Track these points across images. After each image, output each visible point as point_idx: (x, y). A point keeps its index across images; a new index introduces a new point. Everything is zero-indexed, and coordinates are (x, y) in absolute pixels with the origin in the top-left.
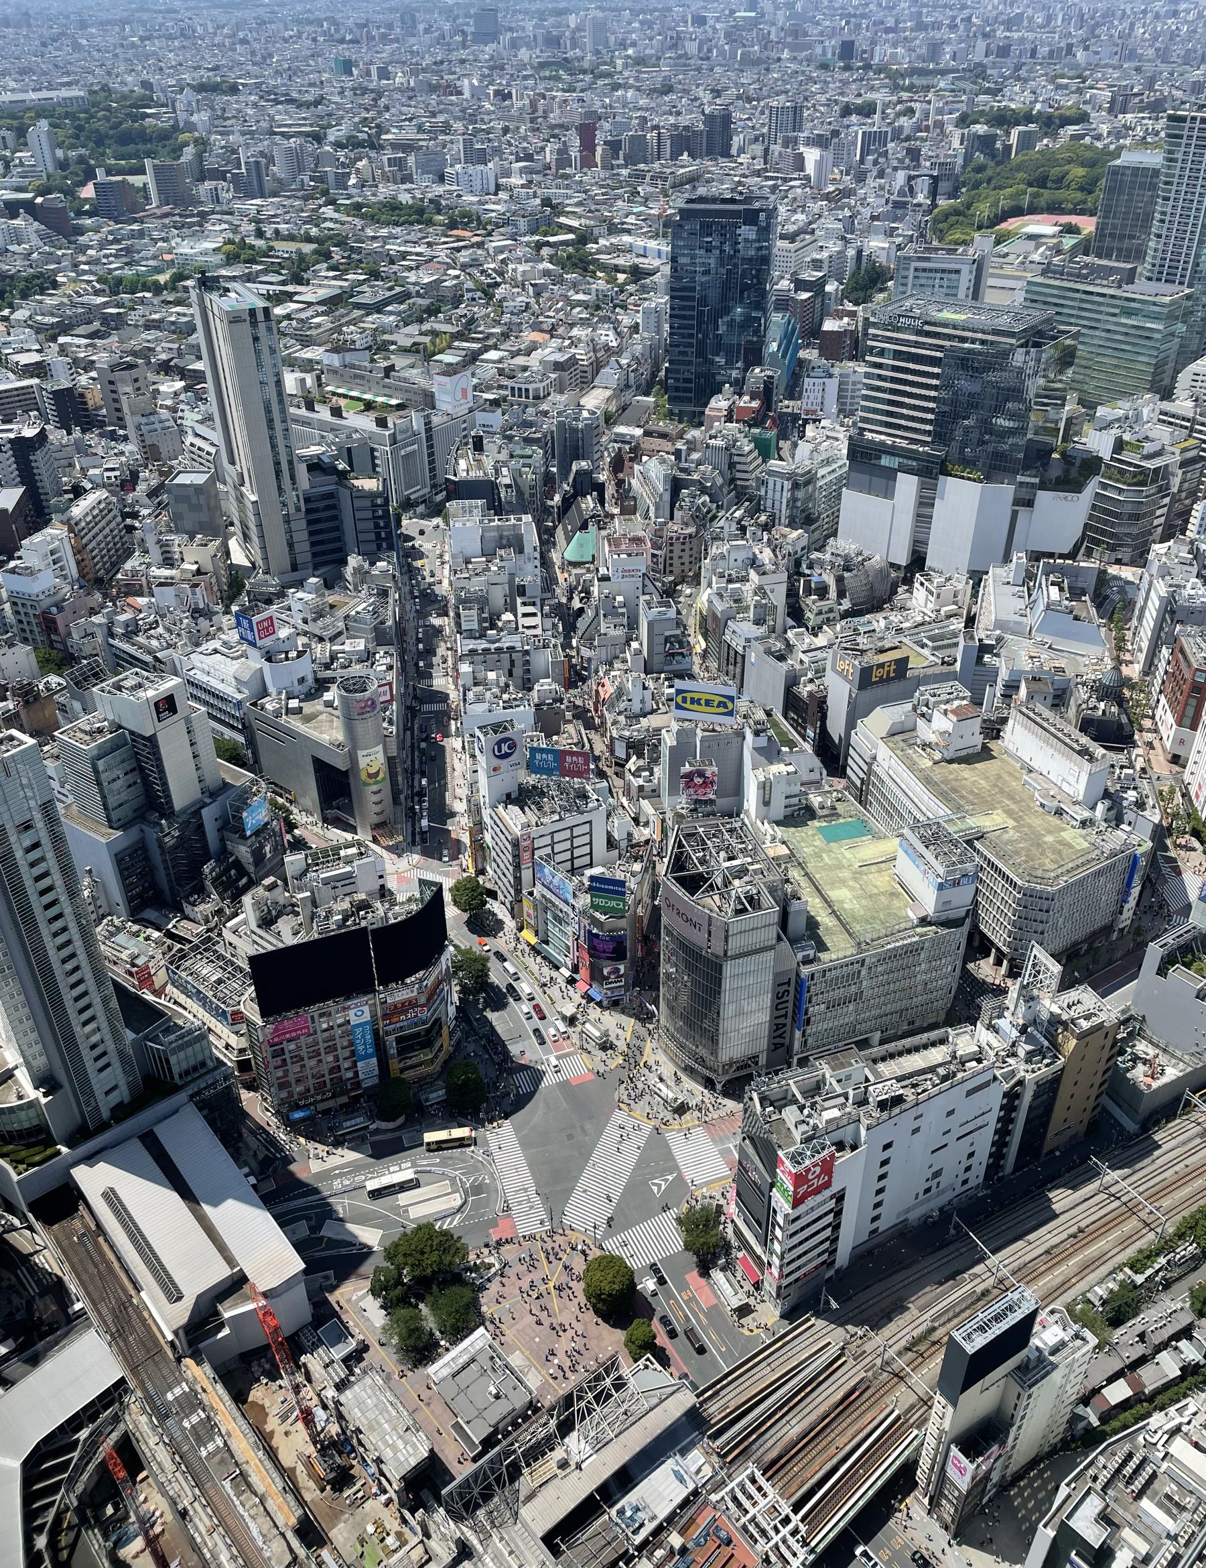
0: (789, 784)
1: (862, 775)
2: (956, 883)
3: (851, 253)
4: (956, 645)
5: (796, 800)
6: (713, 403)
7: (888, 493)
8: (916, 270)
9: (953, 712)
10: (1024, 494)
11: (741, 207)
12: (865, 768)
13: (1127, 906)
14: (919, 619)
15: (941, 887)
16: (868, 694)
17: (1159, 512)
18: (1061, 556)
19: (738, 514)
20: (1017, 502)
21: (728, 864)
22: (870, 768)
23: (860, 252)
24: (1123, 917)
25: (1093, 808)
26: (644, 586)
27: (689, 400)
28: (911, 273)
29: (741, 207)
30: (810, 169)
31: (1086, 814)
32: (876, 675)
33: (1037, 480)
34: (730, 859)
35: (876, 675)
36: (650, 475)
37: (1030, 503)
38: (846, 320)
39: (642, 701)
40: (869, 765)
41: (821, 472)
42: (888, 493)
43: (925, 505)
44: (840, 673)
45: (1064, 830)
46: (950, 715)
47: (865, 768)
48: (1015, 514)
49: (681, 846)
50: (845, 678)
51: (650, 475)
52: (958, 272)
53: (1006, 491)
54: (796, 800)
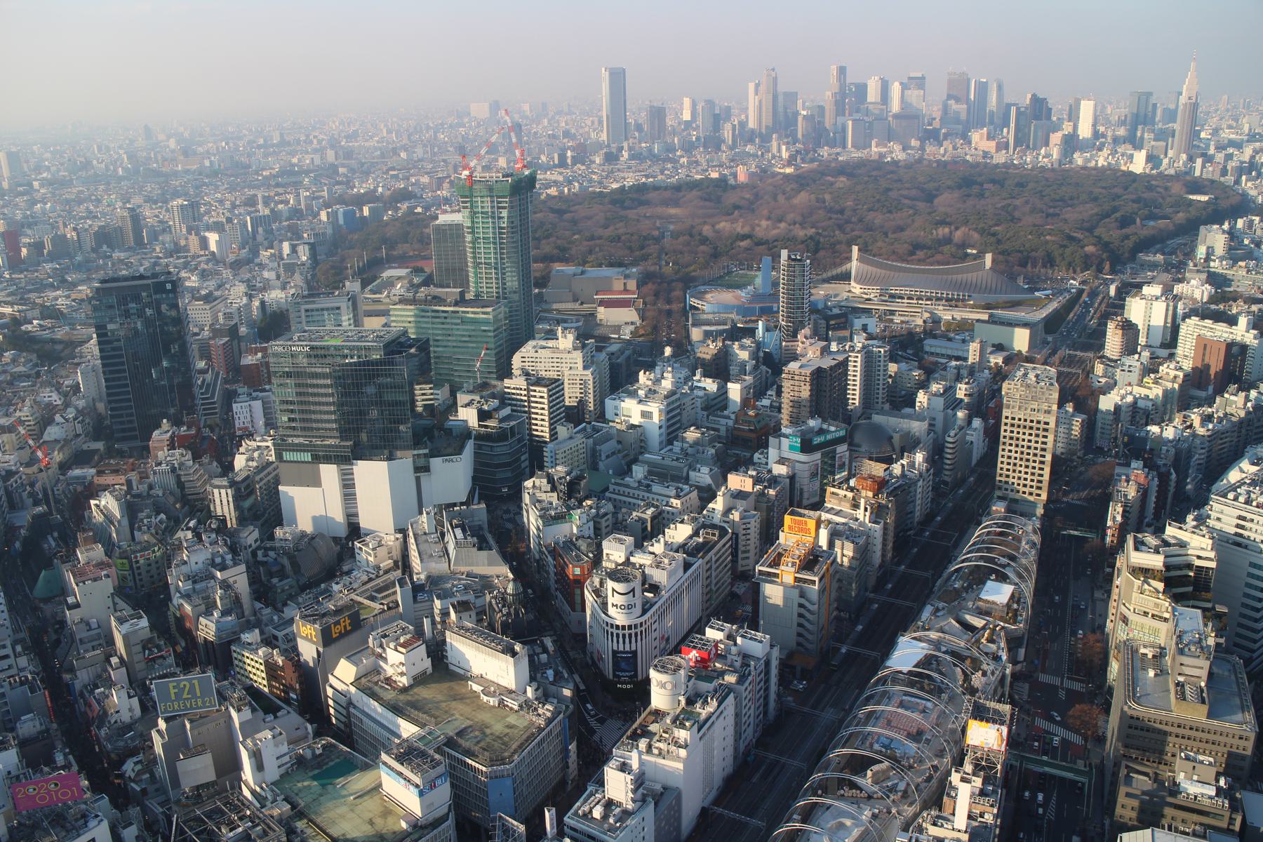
0: (276, 745)
1: (343, 719)
2: (432, 786)
3: (256, 303)
4: (395, 593)
5: (287, 759)
6: (156, 434)
7: (316, 482)
8: (307, 311)
9: (402, 645)
10: (422, 462)
11: (149, 282)
12: (344, 712)
13: (570, 761)
14: (365, 578)
15: (421, 794)
16: (333, 648)
17: (523, 458)
18: (462, 504)
19: (192, 524)
20: (417, 469)
21: (231, 834)
22: (348, 712)
23: (263, 303)
24: (570, 770)
25: (525, 692)
26: (115, 604)
27: (135, 438)
28: (303, 314)
29: (149, 282)
30: (213, 247)
31: (522, 699)
32: (335, 632)
33: (426, 451)
34: (231, 830)
35: (335, 632)
36: (107, 504)
37: (427, 469)
38: (260, 355)
39: (131, 710)
40: (347, 709)
41: (257, 478)
42: (316, 482)
43: (348, 486)
44: (306, 638)
45: (507, 716)
46: (400, 649)
47: (344, 712)
48: (418, 480)
49: (182, 832)
50: (311, 641)
51: (107, 504)
52: (338, 308)
53: (406, 461)
54: (287, 759)
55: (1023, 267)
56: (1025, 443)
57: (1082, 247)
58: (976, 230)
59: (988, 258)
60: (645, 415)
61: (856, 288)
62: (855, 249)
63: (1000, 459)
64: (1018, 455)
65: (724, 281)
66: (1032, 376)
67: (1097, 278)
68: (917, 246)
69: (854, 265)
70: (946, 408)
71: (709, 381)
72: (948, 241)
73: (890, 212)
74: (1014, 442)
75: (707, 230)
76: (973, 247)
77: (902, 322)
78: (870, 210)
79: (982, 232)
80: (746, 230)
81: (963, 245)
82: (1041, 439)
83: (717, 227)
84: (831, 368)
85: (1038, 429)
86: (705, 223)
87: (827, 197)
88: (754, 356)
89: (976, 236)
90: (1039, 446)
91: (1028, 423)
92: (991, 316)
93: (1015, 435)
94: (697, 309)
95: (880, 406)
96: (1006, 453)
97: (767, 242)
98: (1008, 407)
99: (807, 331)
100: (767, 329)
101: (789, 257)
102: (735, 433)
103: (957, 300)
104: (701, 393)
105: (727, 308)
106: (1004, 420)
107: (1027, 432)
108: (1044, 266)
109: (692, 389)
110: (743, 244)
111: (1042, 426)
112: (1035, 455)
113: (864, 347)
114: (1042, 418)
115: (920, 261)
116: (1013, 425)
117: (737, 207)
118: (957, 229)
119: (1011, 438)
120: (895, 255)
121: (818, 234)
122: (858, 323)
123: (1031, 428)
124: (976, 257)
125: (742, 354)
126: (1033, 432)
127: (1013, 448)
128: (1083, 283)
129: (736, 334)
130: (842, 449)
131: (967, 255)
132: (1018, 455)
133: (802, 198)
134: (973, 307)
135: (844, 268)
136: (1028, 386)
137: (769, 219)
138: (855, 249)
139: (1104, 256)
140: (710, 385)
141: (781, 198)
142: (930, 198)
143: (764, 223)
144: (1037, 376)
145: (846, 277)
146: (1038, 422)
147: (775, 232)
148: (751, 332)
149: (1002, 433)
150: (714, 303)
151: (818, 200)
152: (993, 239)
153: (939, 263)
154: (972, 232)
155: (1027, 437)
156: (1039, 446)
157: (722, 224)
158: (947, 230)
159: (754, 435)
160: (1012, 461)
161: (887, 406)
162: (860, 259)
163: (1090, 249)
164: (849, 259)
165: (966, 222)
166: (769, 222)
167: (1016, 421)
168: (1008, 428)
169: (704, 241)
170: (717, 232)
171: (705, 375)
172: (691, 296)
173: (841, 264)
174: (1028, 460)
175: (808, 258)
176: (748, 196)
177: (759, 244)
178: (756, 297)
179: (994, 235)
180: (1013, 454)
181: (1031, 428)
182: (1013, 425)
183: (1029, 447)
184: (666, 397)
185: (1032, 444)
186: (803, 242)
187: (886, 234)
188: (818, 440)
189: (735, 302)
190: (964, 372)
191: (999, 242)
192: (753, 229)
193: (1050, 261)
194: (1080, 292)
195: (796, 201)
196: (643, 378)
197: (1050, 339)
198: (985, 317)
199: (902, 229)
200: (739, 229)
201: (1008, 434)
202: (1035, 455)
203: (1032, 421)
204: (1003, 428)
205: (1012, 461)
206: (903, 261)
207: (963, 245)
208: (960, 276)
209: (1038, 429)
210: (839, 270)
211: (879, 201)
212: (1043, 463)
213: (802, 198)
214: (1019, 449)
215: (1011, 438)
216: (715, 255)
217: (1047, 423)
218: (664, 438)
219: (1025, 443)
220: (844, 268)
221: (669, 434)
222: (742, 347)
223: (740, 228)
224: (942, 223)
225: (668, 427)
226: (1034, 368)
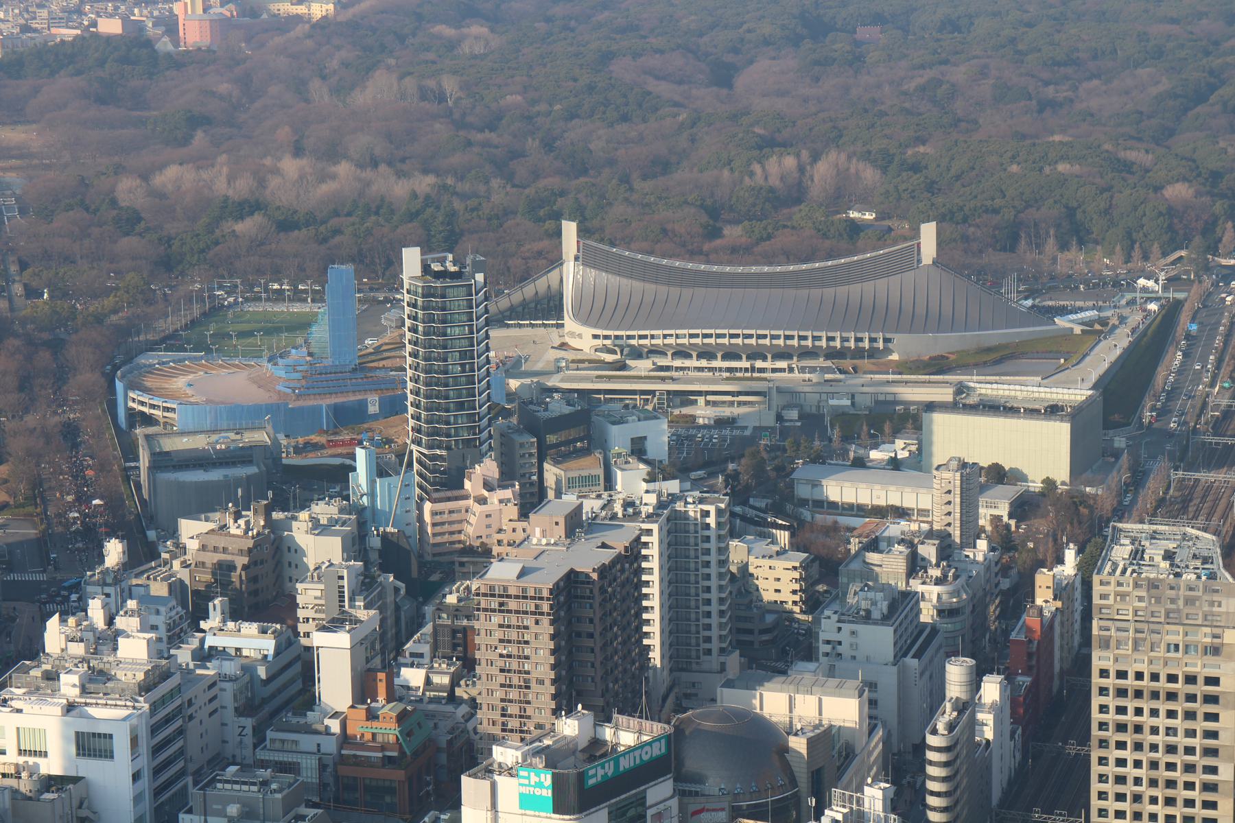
55: (1015, 251)
56: (1160, 739)
57: (1158, 189)
58: (867, 156)
59: (928, 234)
60: (91, 745)
61: (582, 338)
62: (570, 229)
63: (1096, 787)
64: (1142, 773)
65: (203, 337)
66: (1155, 552)
67: (1207, 268)
68: (715, 215)
69: (571, 275)
70: (901, 653)
71: (250, 628)
72: (795, 194)
73: (625, 118)
74: (1128, 737)
75: (128, 190)
76: (865, 204)
77: (721, 423)
78: (572, 116)
79: (884, 162)
80: (243, 187)
81: (840, 197)
82: (1201, 725)
83: (159, 180)
84: (603, 571)
85: (1191, 698)
86: (119, 170)
87: (450, 85)
88: (356, 546)
89: (870, 174)
90: (1197, 742)
91: (1163, 685)
92: (961, 389)
93: (1130, 718)
94: (148, 420)
95: (714, 661)
96: (1111, 770)
97: (310, 220)
98: (1105, 644)
99: (488, 468)
100: (380, 471)
101: (426, 268)
102: (344, 771)
103: (859, 353)
104: (230, 668)
105: (249, 415)
106: (1096, 681)
107: (1163, 706)
108: (1064, 246)
109: (204, 655)
110: (246, 227)
111: (1200, 689)
112: (1189, 768)
113: (661, 505)
114: (1200, 666)
115: (737, 253)
116: (1122, 693)
117: (196, 121)
118: (815, 157)
119: (1121, 727)
120: (663, 238)
121: (445, 187)
122: (619, 438)
123: (1172, 696)
124: (884, 236)
125: (318, 543)
126: (1180, 706)
127: (1126, 754)
128: (1172, 281)
129: (290, 483)
130: (660, 792)
131: (855, 228)
132: (1142, 773)
133: (380, 89)
134: (905, 367)
135: (541, 284)
136: (1153, 585)
137: (298, 151)
138: (570, 229)
139: (1219, 207)
140: (253, 642)
141: (319, 91)
142: (723, 76)
143: (290, 166)
144: (1169, 556)
145: (548, 308)
146: (1190, 679)
147: (326, 188)
148: (335, 478)
149: (1096, 716)
150: (190, 401)
151: (423, 95)
152: (917, 179)
153: (790, 257)
154: (854, 165)
155: (1162, 722)
156: (1197, 742)
157: (172, 172)
158: (790, 162)
159: (399, 775)
160: (1129, 789)
161: (734, 661)
162: (586, 258)
163: (1178, 192)
164: (556, 260)
165: (835, 138)
166: (303, 162)
167: (1130, 682)
168: (1112, 702)
169: (130, 221)
170: (160, 195)
171: (237, 613)
172: (132, 386)
173: (525, 277)
174: (1171, 784)
175: (478, 267)
176: (224, 88)
177: (286, 225)
178: (317, 378)
179: (915, 168)
180: (1130, 771)
181: (1172, 696)
182: (1122, 693)
183: (1171, 749)
184: (145, 688)
185: (1181, 741)
186: (413, 216)
187: (625, 180)
188: (597, 774)
189: (259, 396)
190: (929, 551)
191: (931, 187)
192: (262, 183)
193: (1075, 232)
194: (1172, 311)
195: (362, 98)
196: (55, 634)
197: (1120, 442)
198: (946, 394)
199: (661, 166)
200: (221, 187)
201: (1111, 717)
202: (1189, 768)
203: (1172, 678)
204: (1096, 701)
205: (1129, 789)
206: (693, 254)
207: (840, 197)
208: (868, 286)
209: (1191, 698)
210: (529, 290)
211: (591, 88)
212: (1209, 787)
213: (380, 89)
214: (1145, 756)
215: (1121, 727)
216: (168, 264)
217: (1213, 681)
218: (147, 805)
219: (1160, 739)
220: (541, 284)
221: (157, 792)
222: (317, 527)
223: (222, 181)
224: (769, 144)
225: (157, 771)
226: (1153, 536)
